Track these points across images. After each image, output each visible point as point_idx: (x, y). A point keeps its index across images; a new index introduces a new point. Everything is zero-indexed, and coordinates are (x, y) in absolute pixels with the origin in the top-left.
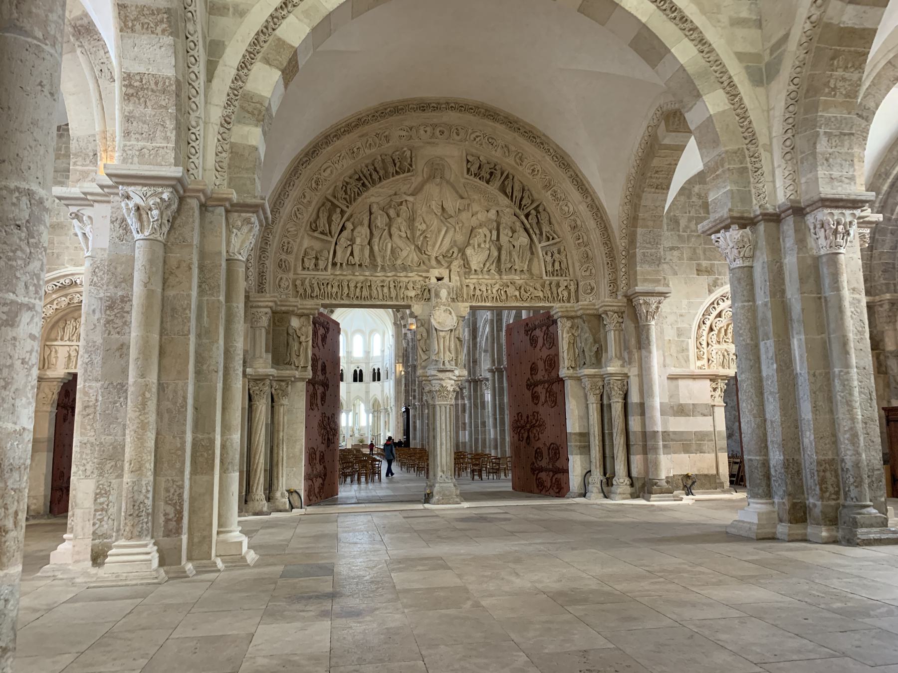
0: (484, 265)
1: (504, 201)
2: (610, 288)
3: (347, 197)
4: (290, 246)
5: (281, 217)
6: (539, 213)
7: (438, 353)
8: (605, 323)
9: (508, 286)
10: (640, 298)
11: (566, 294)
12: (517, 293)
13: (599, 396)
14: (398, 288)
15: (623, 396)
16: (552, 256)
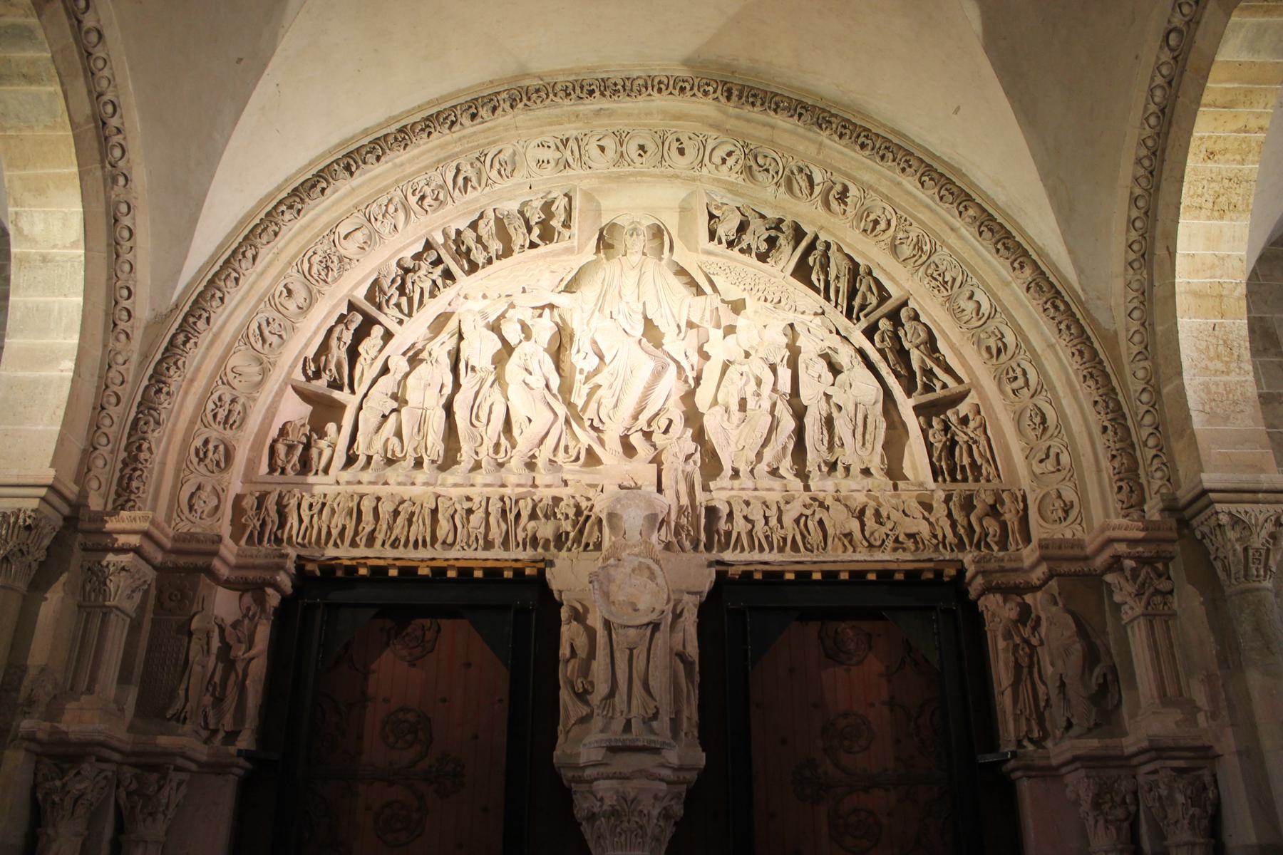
0: (759, 456)
1: (808, 299)
2: (1120, 496)
3: (404, 300)
4: (238, 407)
5: (217, 336)
6: (903, 325)
7: (611, 694)
8: (1117, 598)
9: (828, 509)
10: (1218, 507)
11: (992, 526)
12: (854, 525)
13: (1126, 825)
14: (511, 517)
15: (1205, 823)
16: (946, 428)
